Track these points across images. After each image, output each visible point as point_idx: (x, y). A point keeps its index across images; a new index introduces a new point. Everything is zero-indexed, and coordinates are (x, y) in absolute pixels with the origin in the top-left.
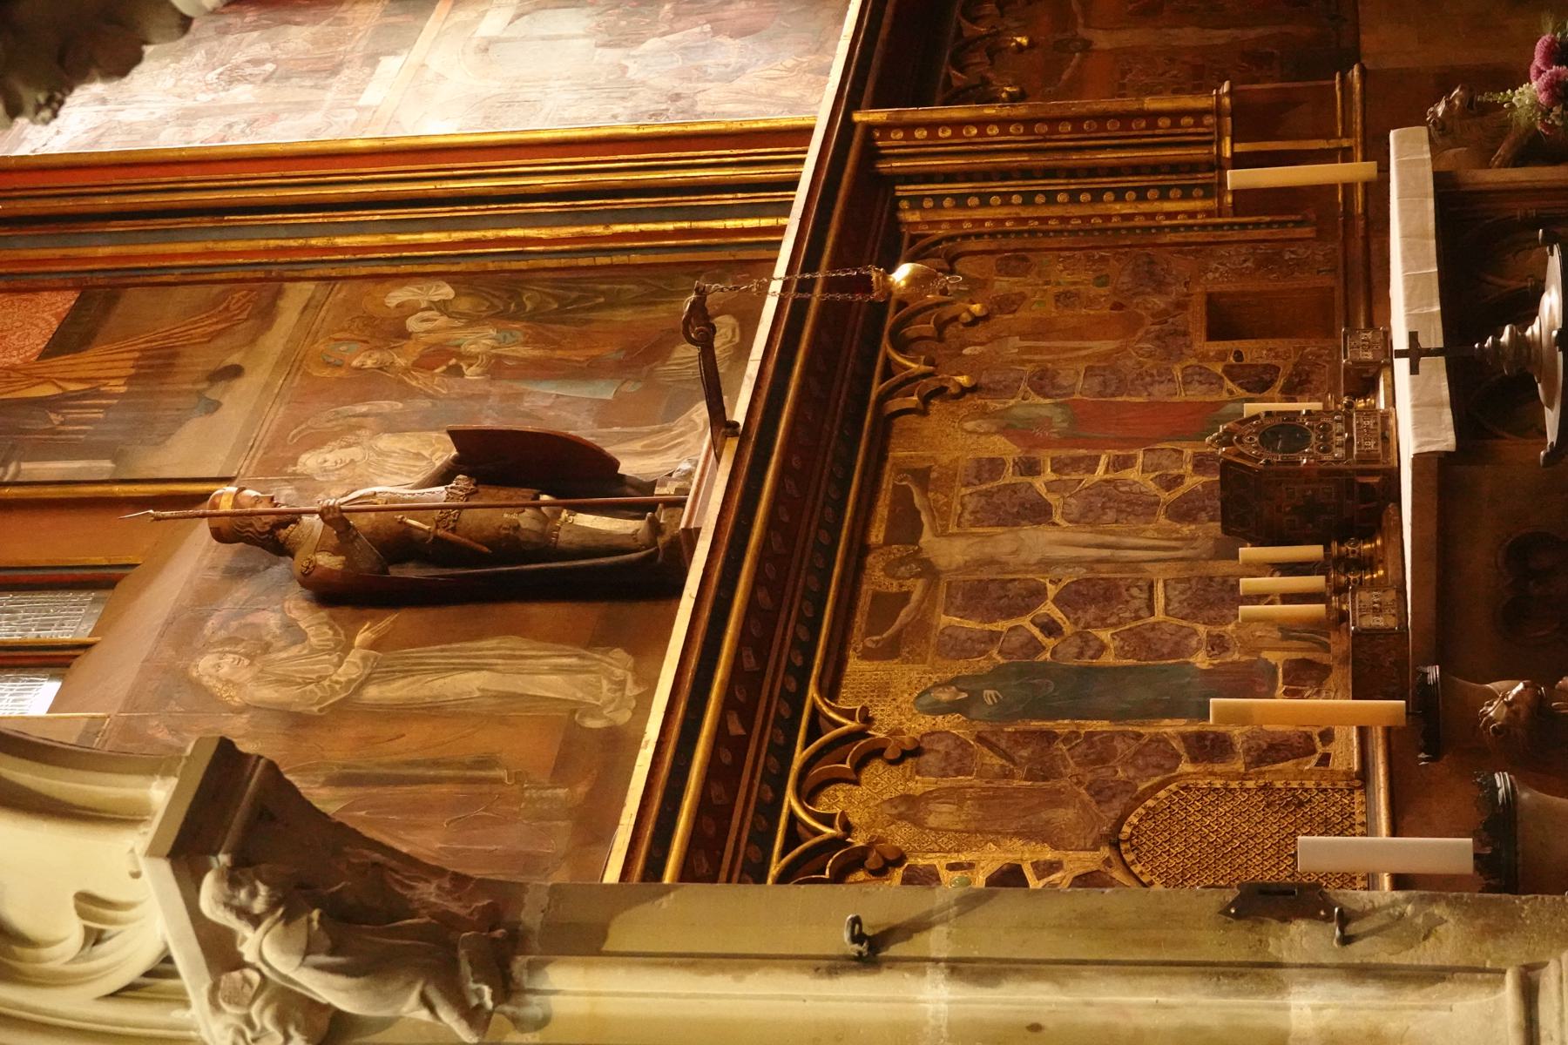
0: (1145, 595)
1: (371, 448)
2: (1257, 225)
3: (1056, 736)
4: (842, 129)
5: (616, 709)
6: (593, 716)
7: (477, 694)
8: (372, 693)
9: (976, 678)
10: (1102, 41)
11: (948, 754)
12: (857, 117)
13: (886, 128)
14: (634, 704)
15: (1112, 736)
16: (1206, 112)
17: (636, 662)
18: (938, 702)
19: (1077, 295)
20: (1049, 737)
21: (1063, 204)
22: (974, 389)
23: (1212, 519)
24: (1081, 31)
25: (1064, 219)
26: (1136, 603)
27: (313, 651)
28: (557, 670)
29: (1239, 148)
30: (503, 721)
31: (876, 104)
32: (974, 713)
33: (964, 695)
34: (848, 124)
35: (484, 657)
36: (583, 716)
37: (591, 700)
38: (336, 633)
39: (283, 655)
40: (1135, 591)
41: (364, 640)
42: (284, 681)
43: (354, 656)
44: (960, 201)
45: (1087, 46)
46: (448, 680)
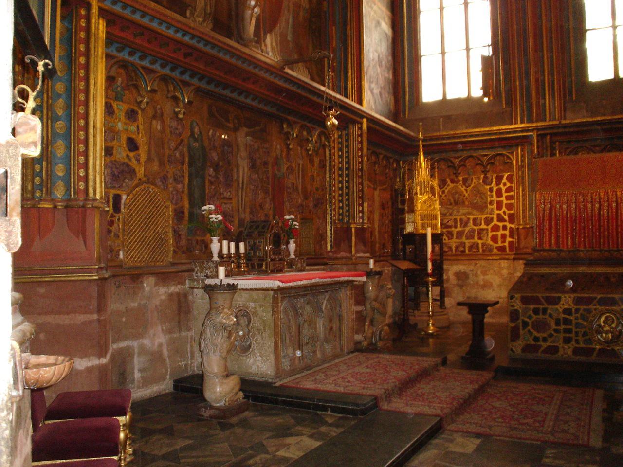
0: (228, 197)
2: (331, 234)
3: (183, 165)
4: (361, 115)
6: (190, 13)
9: (202, 140)
10: (377, 193)
11: (177, 129)
12: (365, 120)
13: (361, 129)
15: (182, 183)
16: (363, 220)
18: (194, 128)
19: (314, 181)
20: (183, 163)
21: (339, 179)
22: (288, 149)
23: (251, 219)
24: (379, 188)
25: (334, 179)
26: (225, 194)
29: (353, 230)
31: (368, 127)
32: (191, 139)
33: (196, 136)
34: (362, 117)
37: (196, 13)
40: (229, 193)
44: (340, 150)
45: (375, 189)
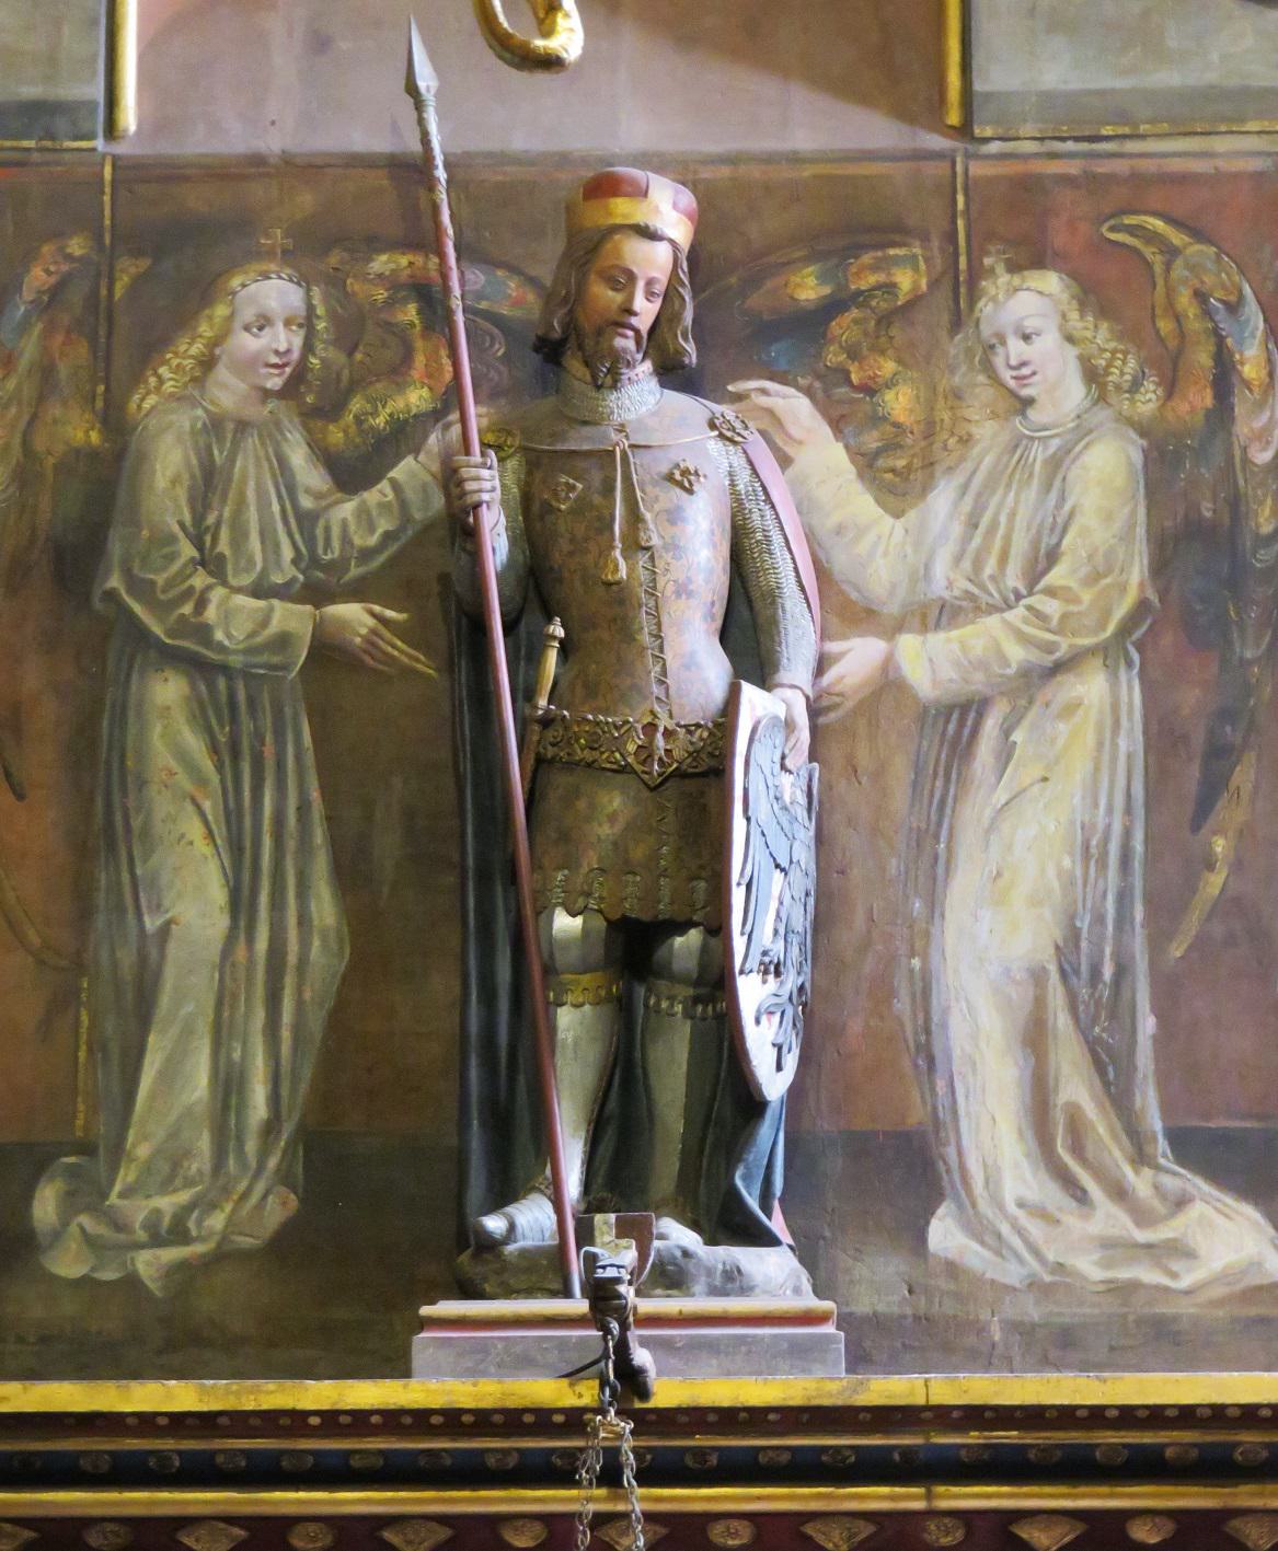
1: (1082, 433)
5: (89, 1240)
7: (151, 923)
8: (168, 690)
14: (109, 1275)
17: (245, 1256)
27: (306, 522)
28: (229, 1086)
30: (63, 1001)
35: (277, 904)
36: (73, 1173)
38: (366, 554)
39: (299, 456)
41: (343, 624)
42: (209, 483)
43: (292, 618)
46: (202, 847)
